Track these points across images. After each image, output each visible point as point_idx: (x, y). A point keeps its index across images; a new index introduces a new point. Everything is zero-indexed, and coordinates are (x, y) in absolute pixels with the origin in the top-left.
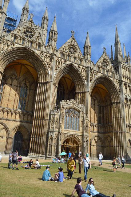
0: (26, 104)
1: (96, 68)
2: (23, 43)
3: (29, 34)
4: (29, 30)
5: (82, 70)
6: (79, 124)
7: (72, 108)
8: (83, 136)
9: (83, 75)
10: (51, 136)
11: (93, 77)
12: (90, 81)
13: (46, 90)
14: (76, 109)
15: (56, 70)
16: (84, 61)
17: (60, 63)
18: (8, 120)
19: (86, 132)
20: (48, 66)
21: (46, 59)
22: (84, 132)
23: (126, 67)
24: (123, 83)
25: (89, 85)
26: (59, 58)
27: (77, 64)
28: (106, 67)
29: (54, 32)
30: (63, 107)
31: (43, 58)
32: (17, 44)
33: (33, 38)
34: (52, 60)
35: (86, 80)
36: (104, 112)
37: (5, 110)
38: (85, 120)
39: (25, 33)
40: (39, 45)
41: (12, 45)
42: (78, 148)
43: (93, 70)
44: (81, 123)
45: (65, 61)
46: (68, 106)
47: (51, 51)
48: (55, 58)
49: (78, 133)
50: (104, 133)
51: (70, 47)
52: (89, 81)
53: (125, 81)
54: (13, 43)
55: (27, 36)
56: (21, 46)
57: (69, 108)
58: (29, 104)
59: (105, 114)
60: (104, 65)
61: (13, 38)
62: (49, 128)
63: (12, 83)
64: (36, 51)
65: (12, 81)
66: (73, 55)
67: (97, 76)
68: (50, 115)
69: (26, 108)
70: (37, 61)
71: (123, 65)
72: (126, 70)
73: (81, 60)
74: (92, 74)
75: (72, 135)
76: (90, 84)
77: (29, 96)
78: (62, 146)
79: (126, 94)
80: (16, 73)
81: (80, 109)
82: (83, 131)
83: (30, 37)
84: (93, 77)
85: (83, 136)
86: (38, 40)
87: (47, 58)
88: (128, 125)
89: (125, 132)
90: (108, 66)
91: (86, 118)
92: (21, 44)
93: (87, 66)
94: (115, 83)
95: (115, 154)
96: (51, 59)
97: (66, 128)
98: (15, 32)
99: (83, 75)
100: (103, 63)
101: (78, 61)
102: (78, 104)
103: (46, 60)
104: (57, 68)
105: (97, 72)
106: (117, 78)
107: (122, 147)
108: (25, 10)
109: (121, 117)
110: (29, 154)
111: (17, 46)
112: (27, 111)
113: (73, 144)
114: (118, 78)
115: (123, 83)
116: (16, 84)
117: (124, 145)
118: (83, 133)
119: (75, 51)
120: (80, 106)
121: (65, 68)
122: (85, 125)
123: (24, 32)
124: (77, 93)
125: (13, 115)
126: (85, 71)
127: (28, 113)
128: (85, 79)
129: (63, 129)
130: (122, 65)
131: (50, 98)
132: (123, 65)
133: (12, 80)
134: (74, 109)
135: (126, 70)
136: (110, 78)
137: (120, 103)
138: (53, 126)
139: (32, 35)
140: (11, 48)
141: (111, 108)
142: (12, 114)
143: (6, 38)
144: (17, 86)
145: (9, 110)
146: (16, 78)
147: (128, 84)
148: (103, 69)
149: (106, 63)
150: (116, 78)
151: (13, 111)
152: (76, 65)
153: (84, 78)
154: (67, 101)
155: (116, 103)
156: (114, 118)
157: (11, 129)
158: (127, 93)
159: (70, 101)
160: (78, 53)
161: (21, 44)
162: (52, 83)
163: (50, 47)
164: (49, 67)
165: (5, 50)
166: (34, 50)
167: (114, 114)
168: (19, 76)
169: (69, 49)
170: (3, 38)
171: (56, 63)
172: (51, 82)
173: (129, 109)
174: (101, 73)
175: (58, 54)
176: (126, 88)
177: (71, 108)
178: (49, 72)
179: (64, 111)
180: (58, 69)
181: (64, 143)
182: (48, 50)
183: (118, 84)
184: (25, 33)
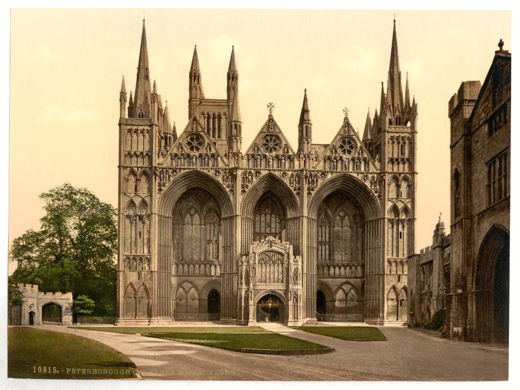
8: (287, 291)
11: (315, 185)
12: (309, 194)
17: (250, 177)
48: (239, 173)
51: (267, 141)
53: (396, 170)
56: (188, 171)
57: (265, 252)
66: (274, 153)
71: (392, 135)
75: (272, 291)
81: (283, 252)
83: (198, 149)
85: (287, 291)
88: (392, 261)
98: (175, 151)
100: (341, 147)
105: (324, 174)
106: (375, 170)
119: (276, 145)
122: (291, 274)
123: (187, 144)
134: (272, 251)
149: (349, 142)
154: (260, 242)
158: (399, 194)
163: (230, 154)
169: (265, 145)
172: (236, 216)
173: (400, 227)
176: (398, 186)
181: (260, 302)
184: (189, 144)
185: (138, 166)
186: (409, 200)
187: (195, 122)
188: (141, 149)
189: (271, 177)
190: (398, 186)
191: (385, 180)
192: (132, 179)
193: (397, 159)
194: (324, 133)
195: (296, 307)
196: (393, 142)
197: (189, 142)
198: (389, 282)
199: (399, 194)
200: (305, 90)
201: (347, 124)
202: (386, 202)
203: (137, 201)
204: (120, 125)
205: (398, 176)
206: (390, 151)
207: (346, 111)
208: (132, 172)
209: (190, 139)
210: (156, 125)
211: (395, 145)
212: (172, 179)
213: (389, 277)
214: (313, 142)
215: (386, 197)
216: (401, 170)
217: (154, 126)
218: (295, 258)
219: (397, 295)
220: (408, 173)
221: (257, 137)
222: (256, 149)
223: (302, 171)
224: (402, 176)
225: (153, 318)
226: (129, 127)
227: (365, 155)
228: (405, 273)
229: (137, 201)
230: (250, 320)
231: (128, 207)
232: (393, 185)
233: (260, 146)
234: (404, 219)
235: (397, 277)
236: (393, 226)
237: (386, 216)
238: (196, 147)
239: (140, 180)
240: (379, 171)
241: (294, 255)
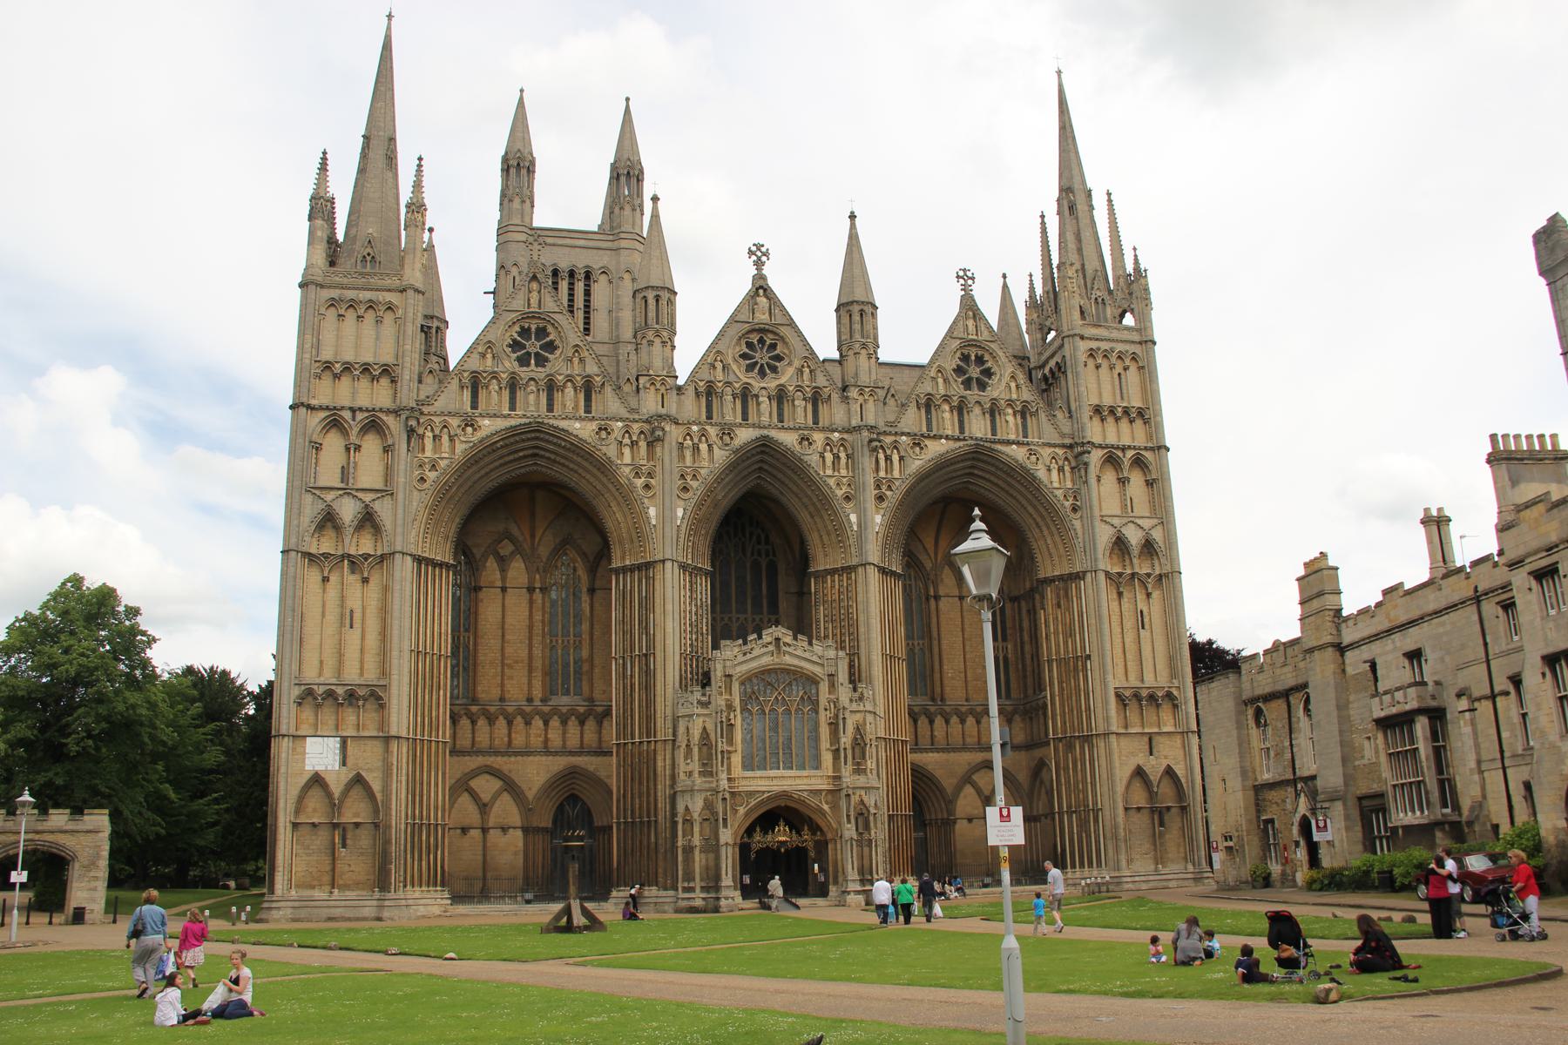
0: (586, 667)
1: (912, 420)
2: (513, 407)
3: (533, 346)
4: (533, 327)
5: (829, 457)
6: (816, 739)
7: (775, 671)
9: (831, 476)
10: (687, 808)
11: (896, 474)
12: (880, 498)
13: (647, 604)
14: (795, 672)
15: (685, 489)
16: (835, 397)
17: (703, 447)
18: (516, 754)
19: (859, 770)
20: (639, 482)
21: (627, 451)
22: (846, 771)
23: (1120, 347)
24: (1095, 457)
25: (870, 524)
26: (695, 428)
27: (795, 429)
28: (982, 386)
29: (651, 295)
30: (730, 676)
31: (611, 451)
32: (487, 422)
33: (557, 365)
34: (658, 449)
35: (849, 506)
36: (1021, 629)
37: (492, 709)
38: (847, 715)
39: (515, 345)
40: (588, 389)
41: (469, 429)
42: (822, 846)
43: (890, 434)
44: (824, 731)
45: (727, 431)
46: (754, 664)
47: (650, 403)
48: (674, 433)
49: (813, 781)
50: (1028, 747)
51: (750, 345)
52: (870, 503)
53: (1112, 439)
54: (469, 423)
55: (523, 361)
56: (513, 422)
57: (763, 672)
58: (597, 661)
59: (1026, 638)
60: (967, 384)
61: (467, 394)
62: (673, 777)
63: (504, 579)
64: (577, 425)
65: (503, 571)
66: (772, 383)
67: (918, 463)
68: (675, 720)
69: (586, 688)
70: (588, 471)
71: (1094, 345)
72: (1119, 369)
73: (816, 399)
74: (888, 458)
75: (785, 795)
76: (878, 519)
77: (592, 625)
78: (744, 849)
79: (1116, 521)
80: (515, 531)
81: (817, 670)
82: (836, 767)
83: (541, 361)
84: (896, 474)
86: (581, 360)
87: (634, 444)
88: (1127, 693)
89: (1106, 735)
90: (995, 379)
91: (854, 706)
92: (506, 412)
93: (854, 423)
94: (1041, 474)
95: (1064, 850)
96: (650, 445)
97: (748, 765)
99: (832, 482)
100: (959, 371)
101: (800, 411)
102: (805, 644)
103: (627, 459)
104: (689, 478)
107: (1096, 811)
108: (513, 171)
109: (1089, 657)
110: (614, 893)
111: (488, 426)
112: (591, 700)
113: (798, 833)
114: (1063, 436)
115: (1095, 457)
116: (523, 580)
117: (1103, 801)
118: (839, 778)
119: (779, 358)
120: (817, 648)
121: (732, 467)
122: (846, 740)
124: (817, 575)
125: (533, 731)
126: (843, 455)
127: (600, 709)
128: (848, 499)
129: (737, 770)
130: (1083, 346)
131: (669, 642)
132: (1094, 345)
133: (503, 562)
135: (1119, 369)
136: (999, 447)
137: (1078, 576)
138: (689, 768)
139: (551, 347)
140: (464, 446)
141: (1033, 613)
142: (528, 723)
143: (439, 405)
144: (531, 590)
145: (510, 710)
146: (518, 550)
147: (1130, 454)
148: (961, 409)
150: (1050, 435)
151: (528, 709)
152: (789, 439)
153: (839, 493)
154: (745, 643)
155: (1061, 578)
156: (1050, 661)
157: (534, 790)
158: (1127, 505)
159: (760, 637)
160: (797, 363)
161: (506, 412)
162: (668, 565)
163: (642, 380)
164: (647, 487)
165: (443, 463)
166: (563, 424)
167: (1053, 645)
168: (533, 536)
169: (744, 356)
170: (426, 410)
171: (682, 457)
172: (663, 561)
173: (1140, 596)
174: (947, 438)
175: (690, 408)
176: (1123, 481)
177: (769, 671)
178: (652, 512)
179: (736, 687)
180: (694, 484)
181: (750, 831)
182: (634, 404)
183: (1061, 469)
185: (357, 404)
186: (1155, 521)
187: (535, 285)
188: (369, 359)
189: (765, 450)
190: (1123, 481)
191: (1086, 464)
192: (333, 444)
193: (1112, 411)
194: (911, 334)
195: (864, 842)
196: (1098, 367)
197: (514, 341)
198: (1119, 760)
199: (1127, 505)
200: (852, 217)
201: (969, 307)
202: (1097, 523)
203: (348, 511)
204: (301, 286)
205: (1120, 454)
206: (1092, 386)
207: (965, 277)
208: (334, 423)
209: (520, 334)
210: (417, 291)
211: (1104, 370)
212: (460, 448)
213: (1124, 741)
214: (884, 355)
215: (1097, 513)
216: (1126, 441)
217: (410, 293)
218: (855, 690)
219: (1152, 795)
220: (1146, 449)
221: (722, 334)
222: (719, 365)
223: (857, 429)
224: (1130, 454)
225: (392, 895)
226: (335, 293)
227: (1026, 395)
228: (1165, 729)
229: (348, 511)
230: (724, 893)
232: (1110, 477)
233: (730, 361)
234: (1149, 575)
235: (1146, 739)
236: (1120, 594)
237: (1102, 566)
238: (537, 354)
239: (358, 448)
240: (1068, 441)
241: (852, 681)
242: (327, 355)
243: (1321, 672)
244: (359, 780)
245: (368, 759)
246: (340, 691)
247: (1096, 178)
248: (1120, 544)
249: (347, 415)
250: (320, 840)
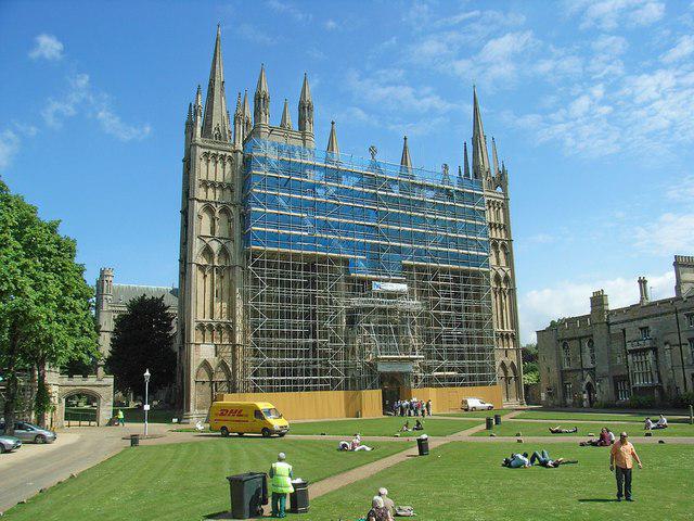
158: (498, 262)
188: (220, 179)
190: (497, 253)
199: (498, 262)
203: (215, 246)
216: (499, 237)
226: (207, 151)
229: (215, 246)
231: (203, 254)
242: (204, 177)
243: (600, 335)
244: (223, 364)
245: (227, 352)
246: (214, 324)
247: (484, 129)
248: (497, 278)
249: (214, 205)
250: (207, 388)
